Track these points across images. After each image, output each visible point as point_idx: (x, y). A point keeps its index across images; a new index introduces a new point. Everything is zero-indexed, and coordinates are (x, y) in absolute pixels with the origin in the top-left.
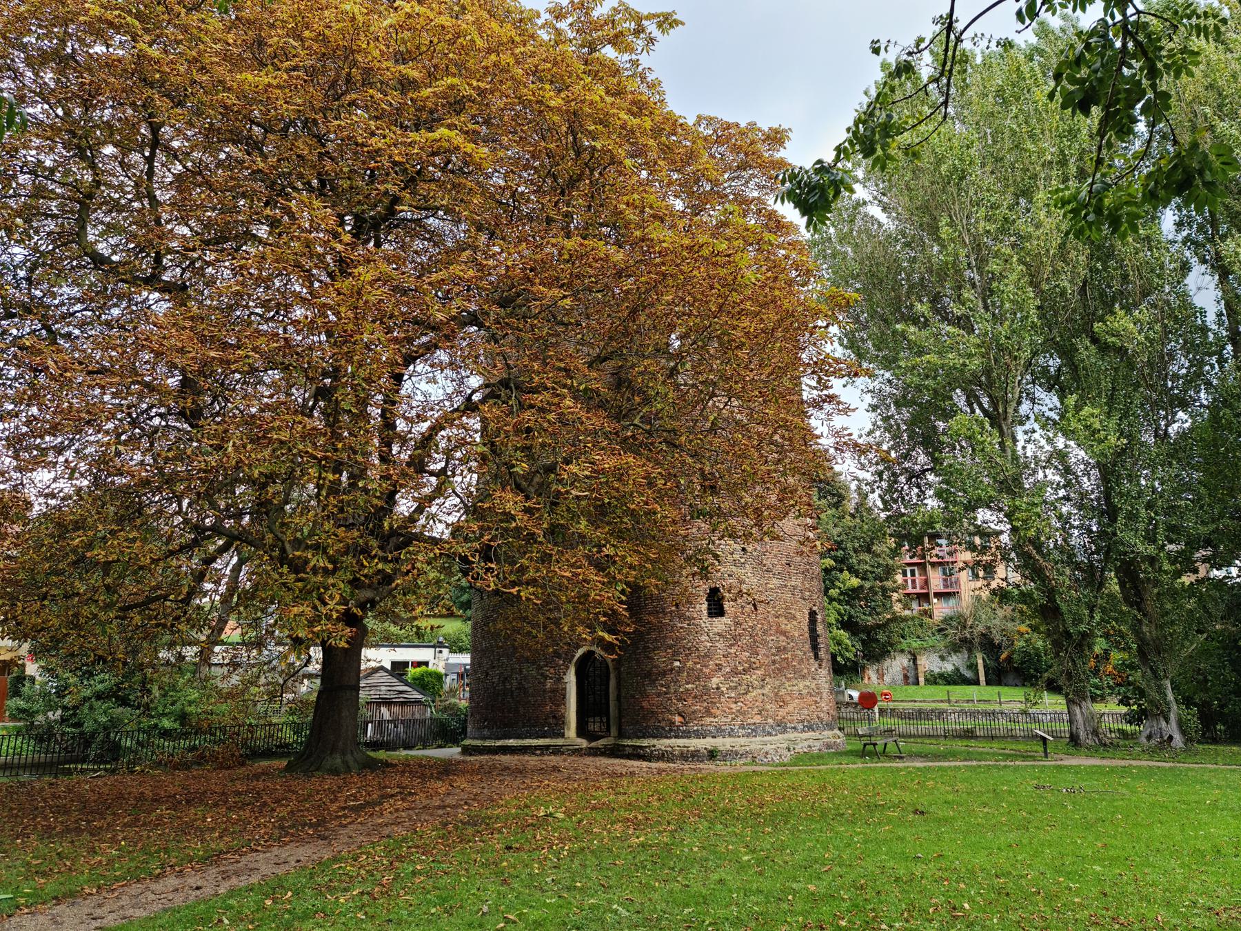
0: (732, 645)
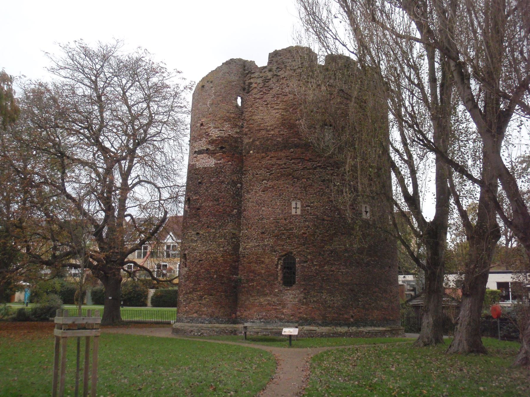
0: (186, 281)
